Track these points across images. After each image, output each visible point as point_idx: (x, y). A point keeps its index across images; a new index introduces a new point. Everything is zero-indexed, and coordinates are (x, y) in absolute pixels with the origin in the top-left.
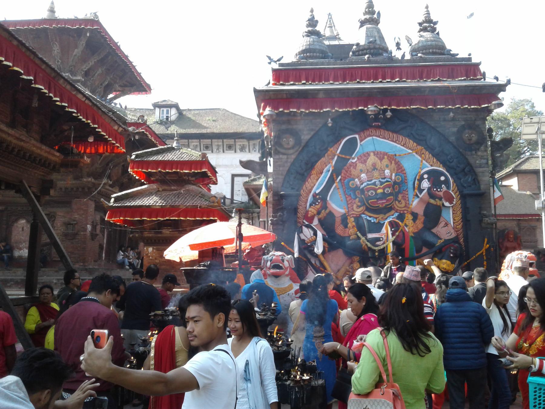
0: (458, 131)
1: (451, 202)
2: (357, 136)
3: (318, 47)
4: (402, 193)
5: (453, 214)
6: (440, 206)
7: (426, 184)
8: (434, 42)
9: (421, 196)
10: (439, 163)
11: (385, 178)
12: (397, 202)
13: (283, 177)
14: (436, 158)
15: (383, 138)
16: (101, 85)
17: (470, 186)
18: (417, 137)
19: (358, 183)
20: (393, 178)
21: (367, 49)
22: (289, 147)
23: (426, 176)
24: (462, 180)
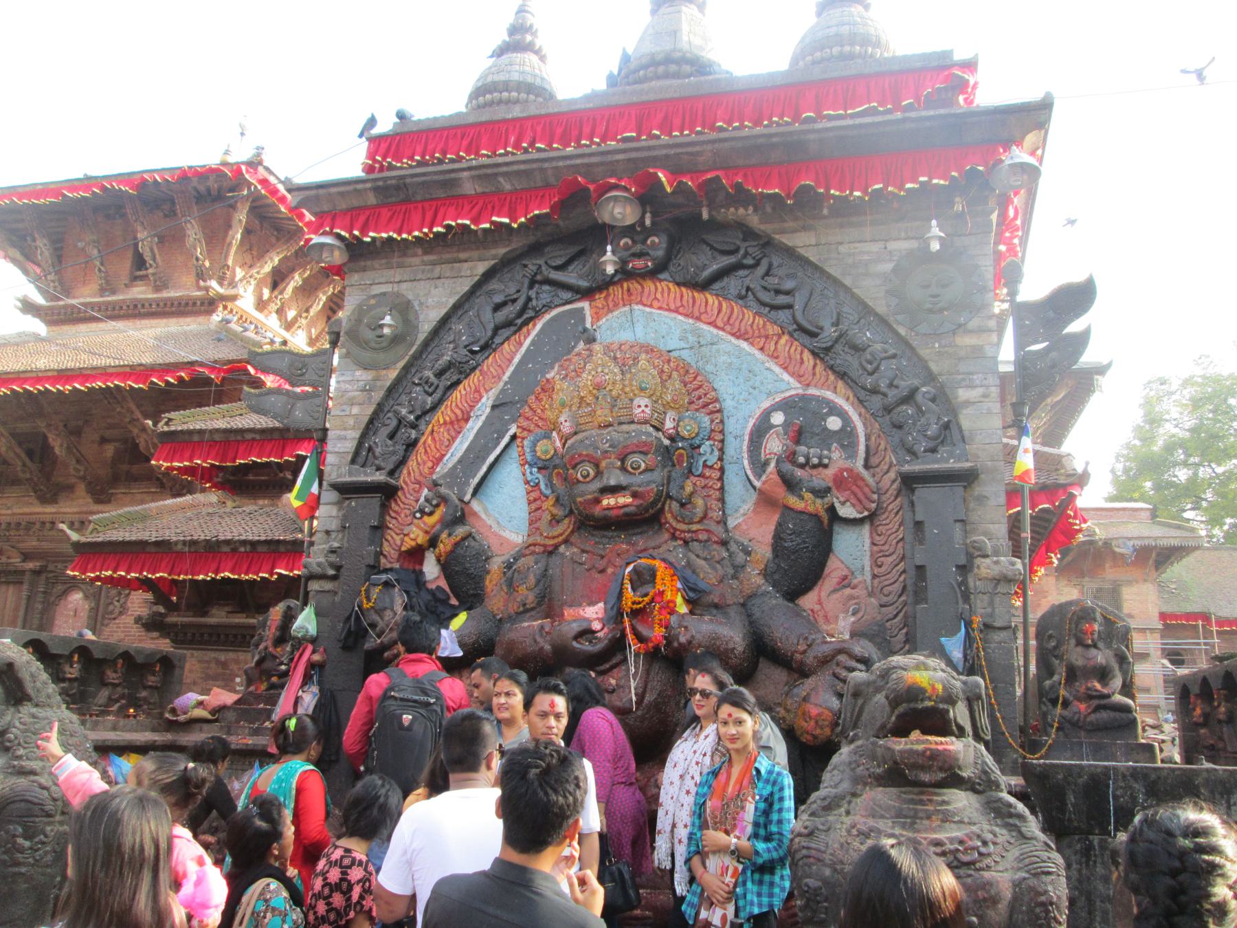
0: (894, 270)
1: (859, 503)
2: (585, 305)
3: (516, 77)
4: (702, 476)
5: (873, 544)
6: (815, 516)
7: (774, 445)
8: (847, 27)
9: (757, 484)
10: (832, 377)
11: (633, 422)
12: (675, 505)
13: (356, 434)
14: (822, 359)
15: (660, 308)
16: (307, 311)
17: (933, 450)
18: (766, 297)
19: (558, 444)
20: (669, 424)
21: (645, 67)
22: (384, 344)
23: (778, 418)
24: (906, 428)
